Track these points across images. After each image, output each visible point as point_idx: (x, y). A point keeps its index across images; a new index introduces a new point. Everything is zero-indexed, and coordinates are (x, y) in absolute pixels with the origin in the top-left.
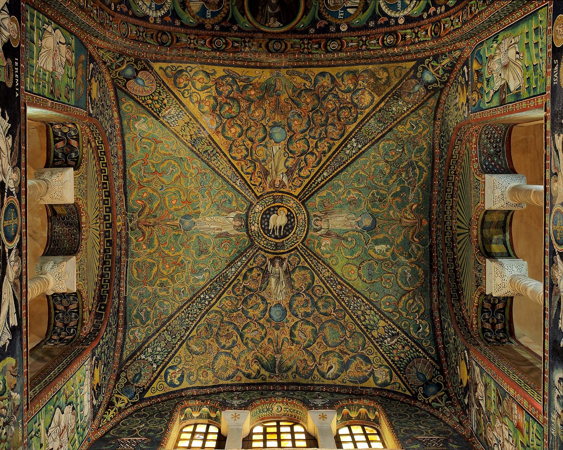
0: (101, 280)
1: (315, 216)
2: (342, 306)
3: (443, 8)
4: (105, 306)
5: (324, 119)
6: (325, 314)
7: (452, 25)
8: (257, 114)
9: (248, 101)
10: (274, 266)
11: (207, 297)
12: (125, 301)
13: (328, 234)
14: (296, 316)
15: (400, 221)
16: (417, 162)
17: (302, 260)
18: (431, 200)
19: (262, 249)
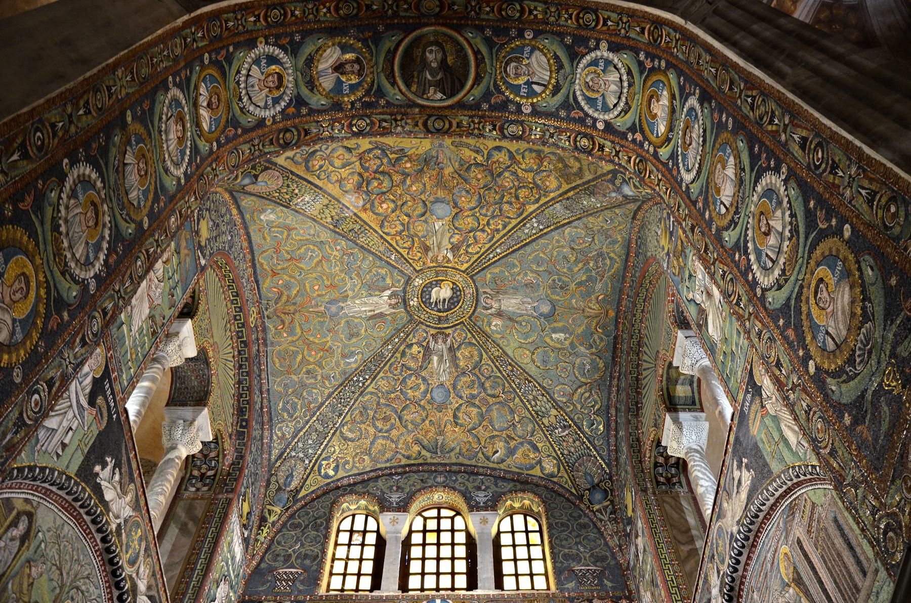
0: (239, 388)
1: (485, 293)
2: (512, 387)
3: (651, 149)
4: (246, 421)
5: (497, 198)
6: (493, 396)
7: (658, 185)
8: (414, 188)
9: (403, 174)
10: (436, 342)
11: (361, 379)
12: (269, 394)
13: (500, 314)
14: (461, 397)
15: (583, 310)
16: (608, 254)
17: (469, 335)
18: (621, 291)
19: (422, 323)
